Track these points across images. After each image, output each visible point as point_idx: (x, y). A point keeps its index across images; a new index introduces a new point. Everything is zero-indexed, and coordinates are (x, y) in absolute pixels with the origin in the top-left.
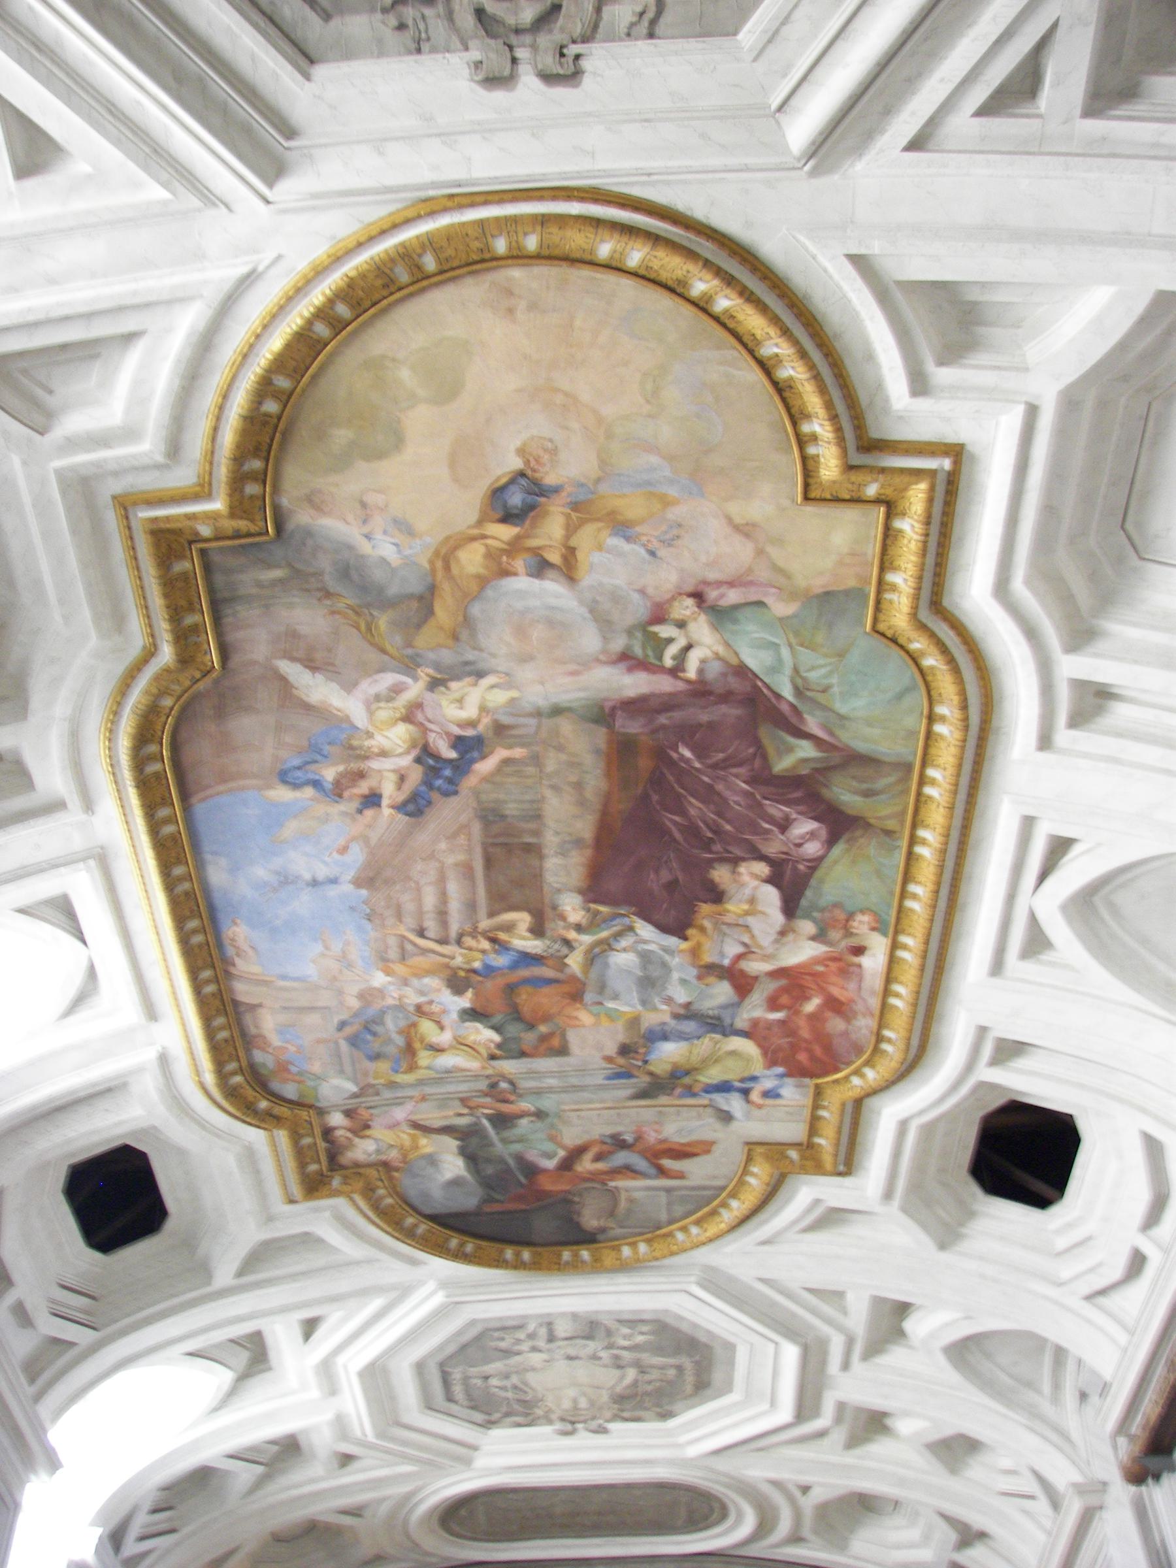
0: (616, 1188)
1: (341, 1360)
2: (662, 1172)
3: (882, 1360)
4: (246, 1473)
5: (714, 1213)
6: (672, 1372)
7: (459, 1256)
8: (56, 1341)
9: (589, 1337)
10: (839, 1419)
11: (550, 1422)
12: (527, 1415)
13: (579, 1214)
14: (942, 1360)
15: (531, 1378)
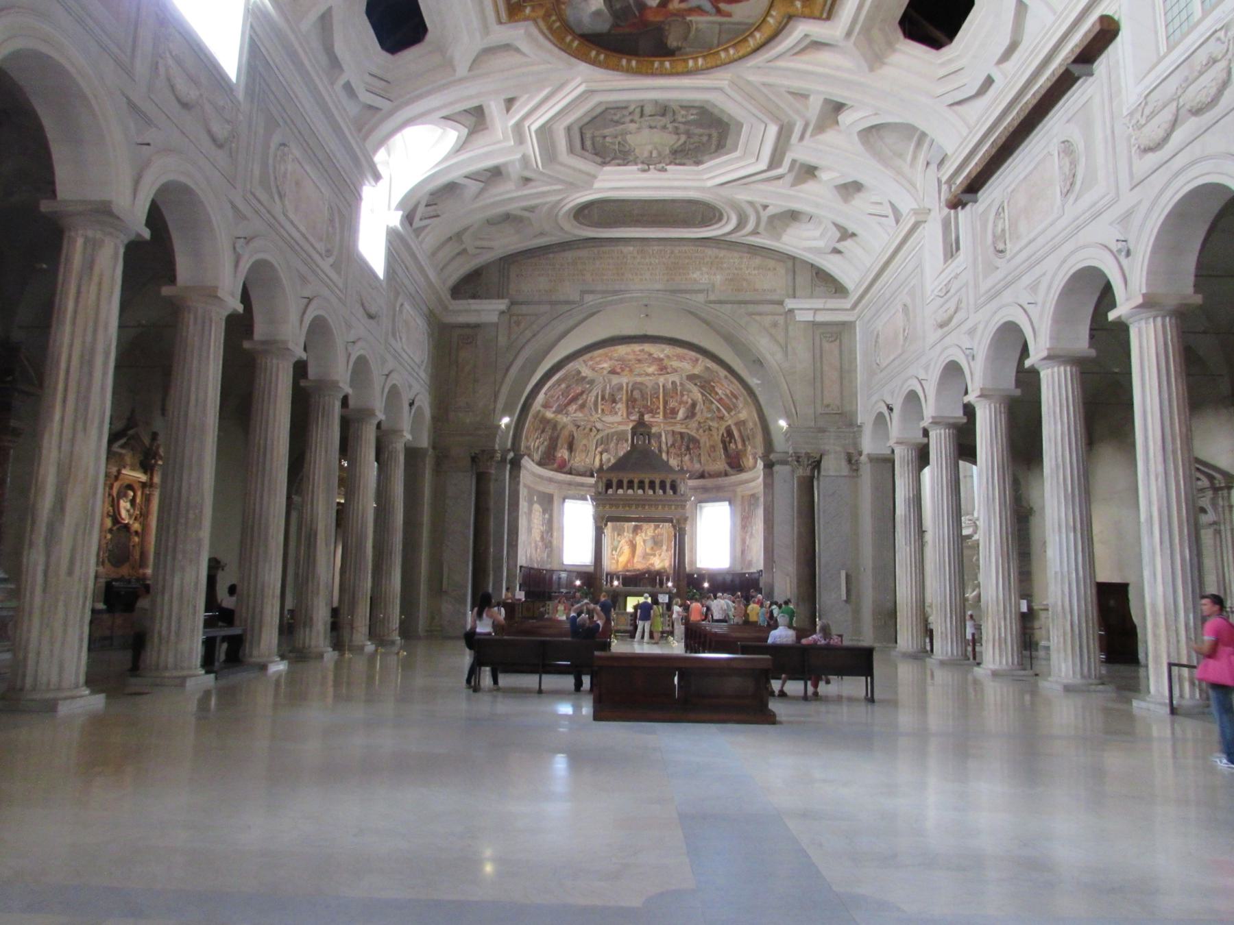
0: (691, 21)
1: (527, 124)
2: (719, 12)
3: (821, 137)
4: (474, 187)
5: (745, 40)
6: (705, 139)
7: (594, 63)
8: (370, 107)
9: (663, 115)
10: (791, 169)
11: (636, 164)
12: (624, 159)
13: (667, 39)
14: (856, 138)
15: (628, 137)
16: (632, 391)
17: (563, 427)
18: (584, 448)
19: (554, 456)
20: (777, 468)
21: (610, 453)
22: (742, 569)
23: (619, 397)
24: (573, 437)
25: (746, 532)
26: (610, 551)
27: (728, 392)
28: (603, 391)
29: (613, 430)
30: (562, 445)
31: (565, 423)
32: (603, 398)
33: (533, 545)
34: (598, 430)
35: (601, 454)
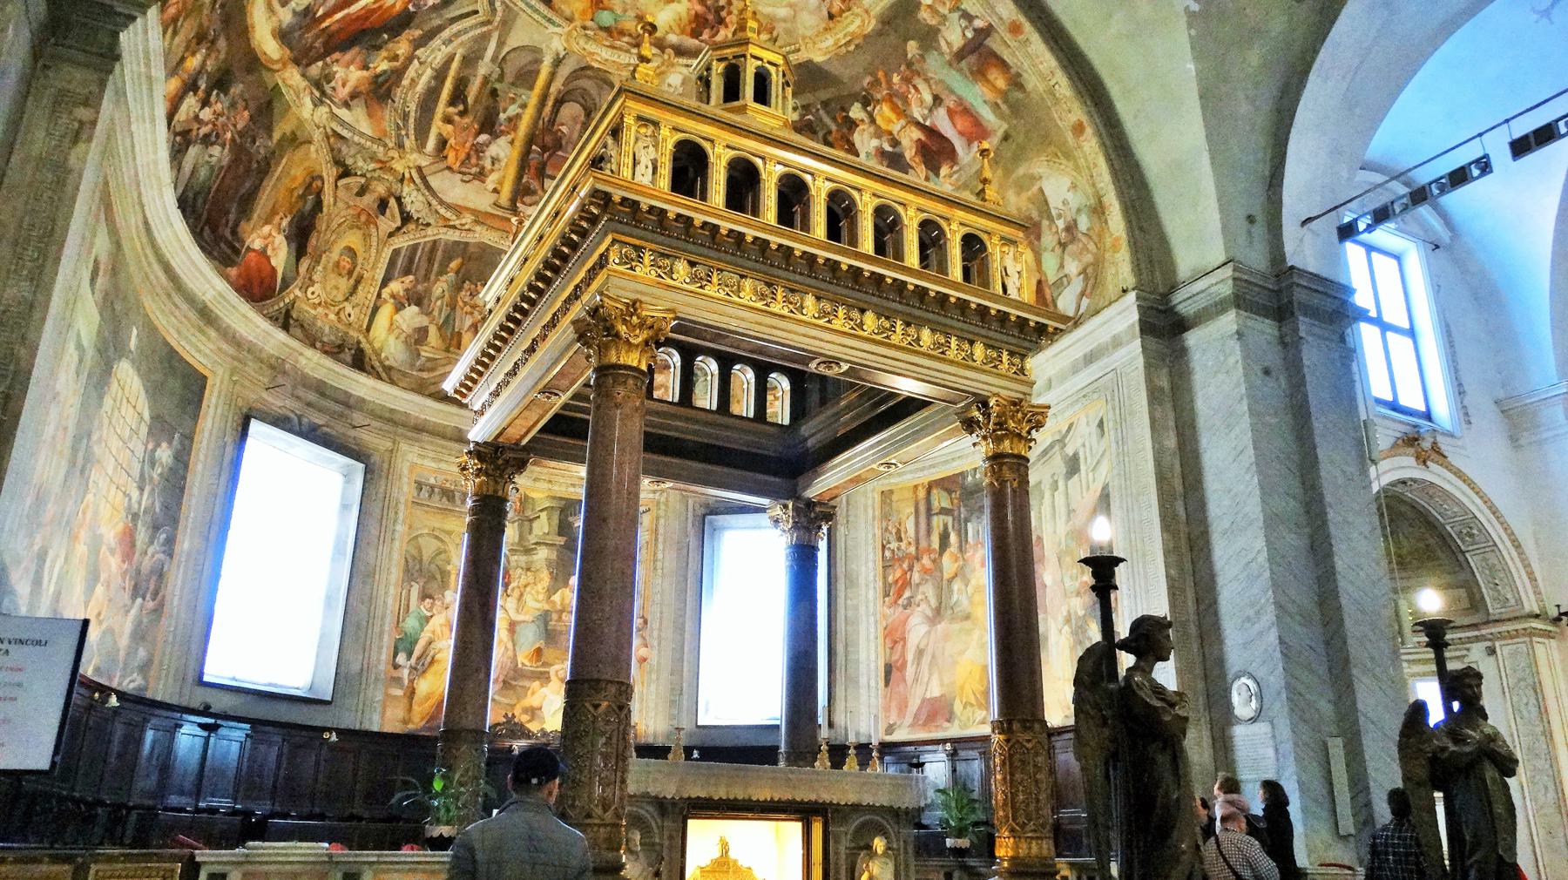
16: (559, 102)
17: (295, 141)
18: (346, 263)
19: (234, 232)
20: (1192, 338)
21: (429, 314)
22: (890, 729)
23: (513, 110)
24: (318, 205)
25: (905, 608)
26: (385, 655)
27: (910, 139)
28: (470, 61)
29: (454, 236)
30: (274, 212)
31: (301, 122)
32: (458, 96)
33: (82, 549)
34: (406, 218)
35: (399, 307)
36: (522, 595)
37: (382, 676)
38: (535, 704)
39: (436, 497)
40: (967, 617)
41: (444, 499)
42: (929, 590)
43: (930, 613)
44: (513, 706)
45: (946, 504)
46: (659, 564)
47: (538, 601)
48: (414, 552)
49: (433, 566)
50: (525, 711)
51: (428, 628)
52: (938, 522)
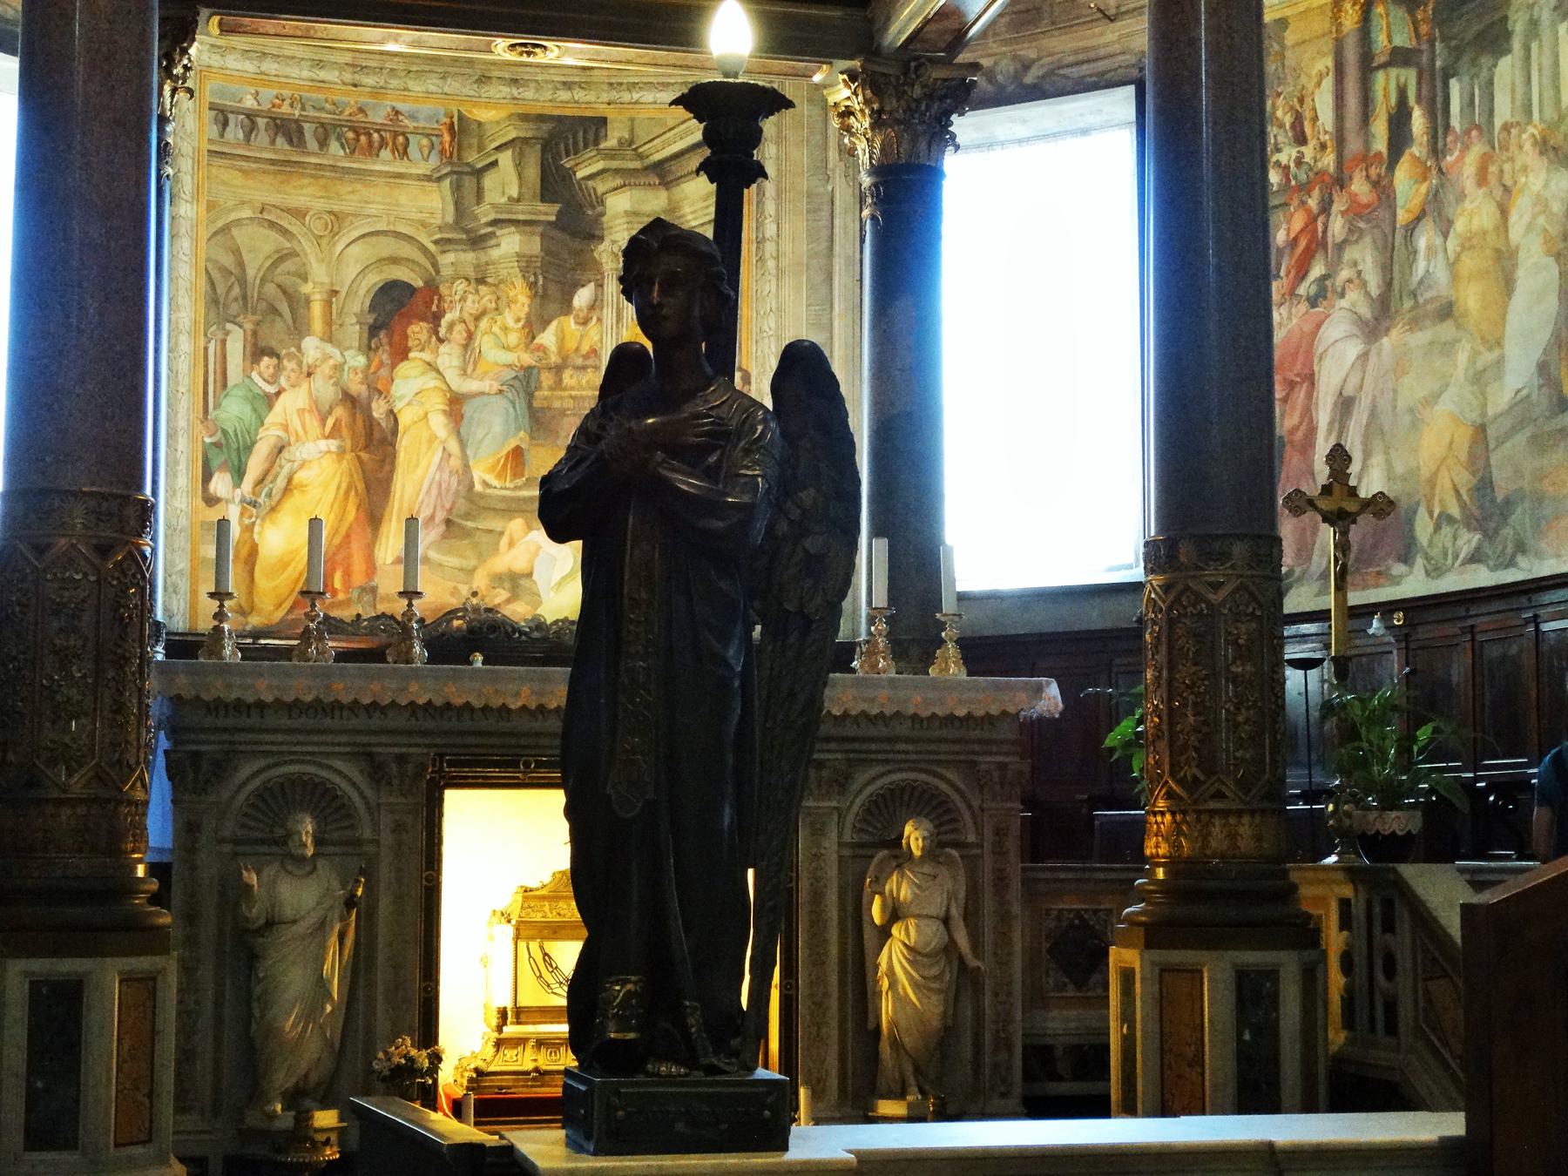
25: (1313, 302)
36: (470, 336)
37: (184, 522)
38: (519, 565)
39: (262, 138)
40: (1447, 311)
41: (281, 142)
42: (1364, 257)
43: (1365, 311)
44: (471, 572)
45: (1403, 39)
46: (770, 248)
47: (506, 348)
48: (228, 261)
49: (271, 289)
50: (498, 579)
51: (274, 417)
52: (1385, 84)
